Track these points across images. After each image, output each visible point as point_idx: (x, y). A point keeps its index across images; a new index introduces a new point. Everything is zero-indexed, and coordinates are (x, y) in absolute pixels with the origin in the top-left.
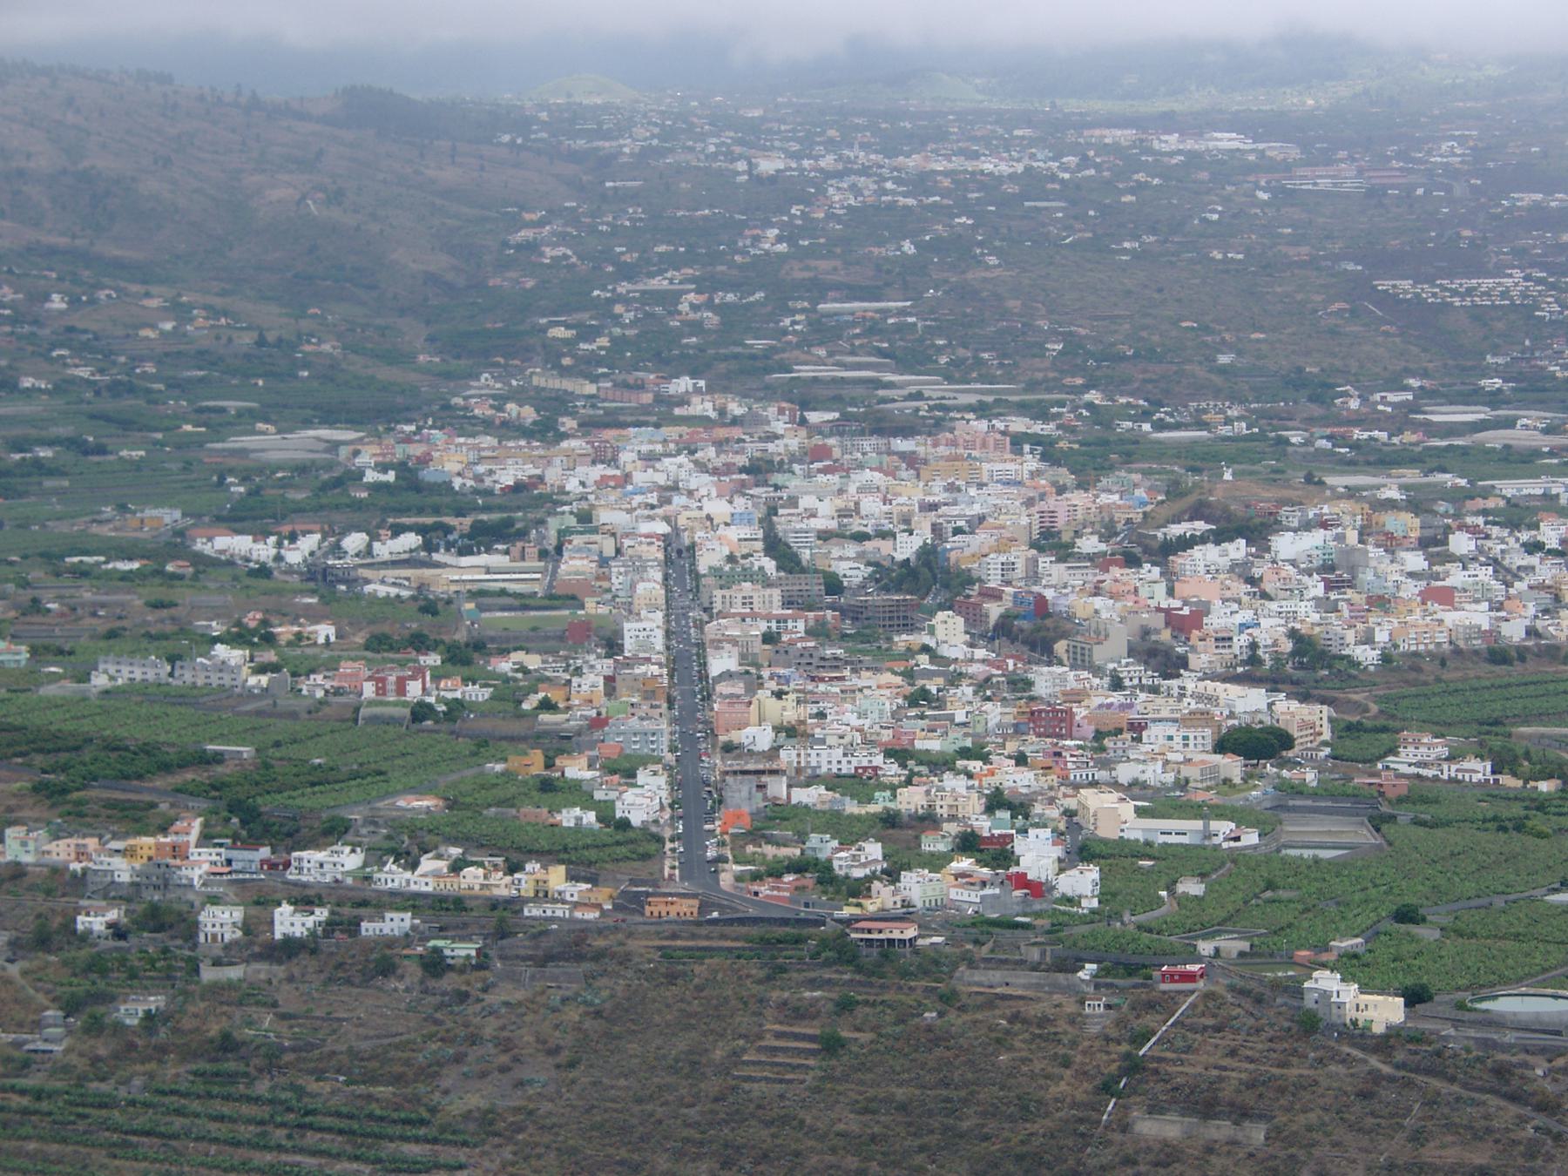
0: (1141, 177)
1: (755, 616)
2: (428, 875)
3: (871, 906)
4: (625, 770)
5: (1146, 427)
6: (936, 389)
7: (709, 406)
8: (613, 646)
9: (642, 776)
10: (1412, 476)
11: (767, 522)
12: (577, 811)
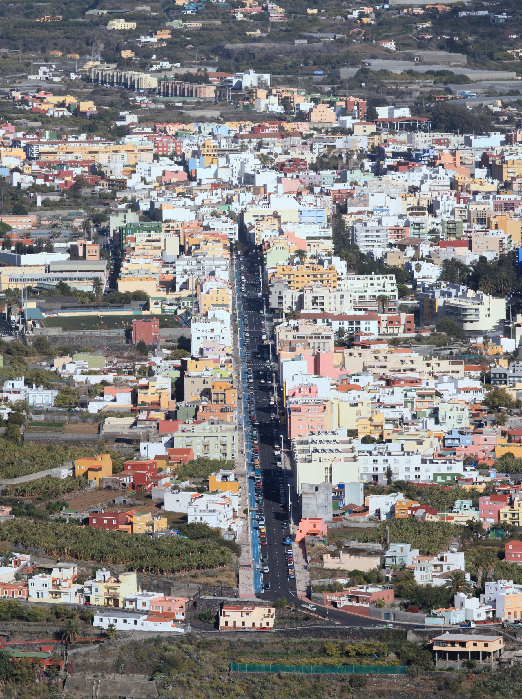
3: (456, 616)
7: (274, 100)
12: (147, 517)
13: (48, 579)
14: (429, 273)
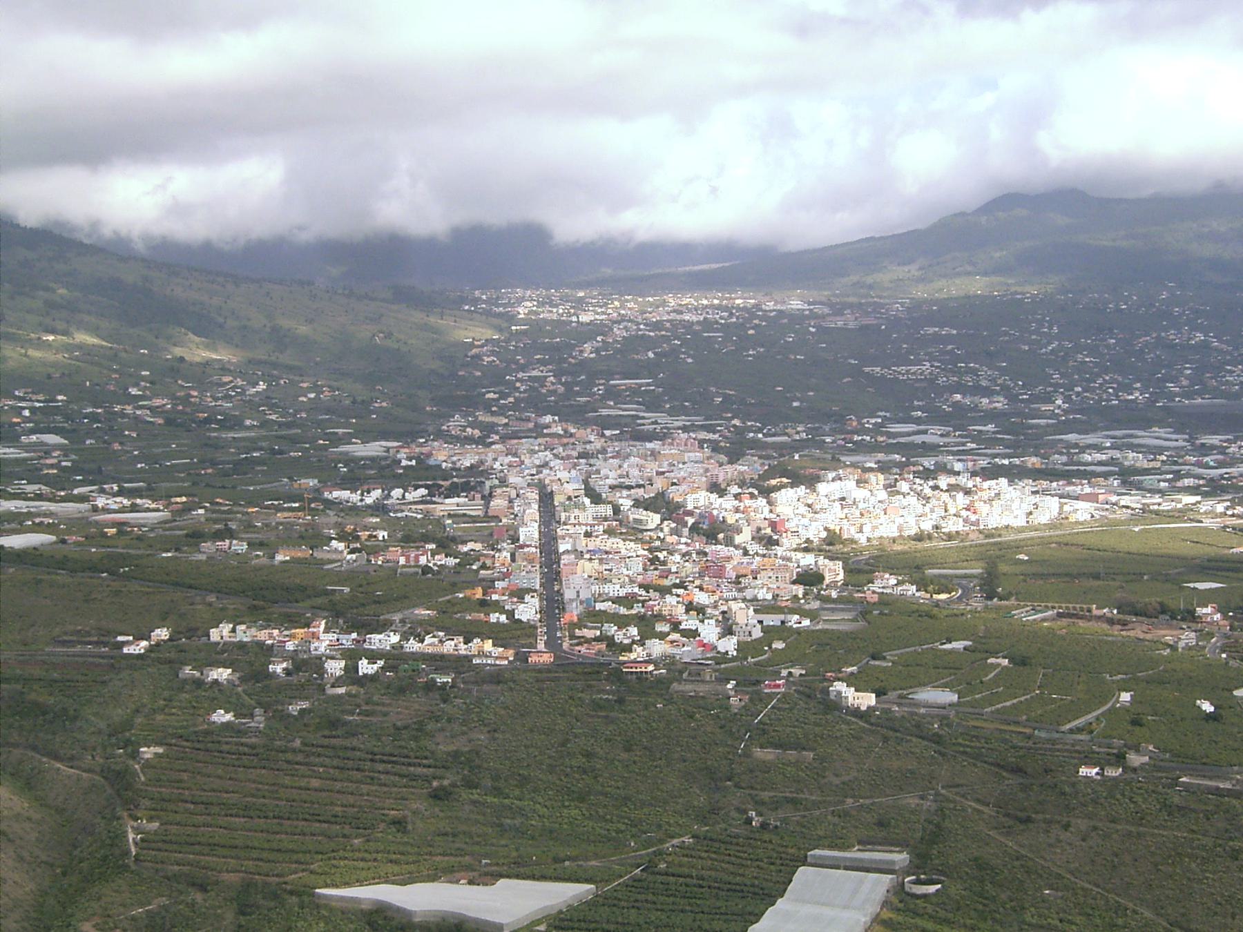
0: (756, 322)
1: (580, 524)
2: (429, 644)
3: (633, 656)
4: (519, 594)
5: (760, 436)
6: (663, 418)
8: (515, 539)
9: (527, 598)
10: (881, 456)
11: (586, 482)
12: (497, 615)
13: (452, 643)
14: (626, 503)
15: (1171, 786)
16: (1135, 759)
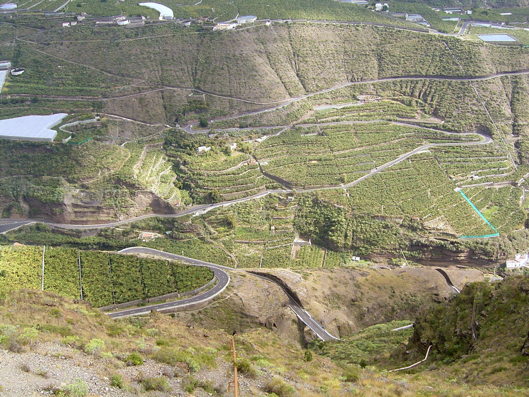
15: (93, 26)
16: (80, 18)
